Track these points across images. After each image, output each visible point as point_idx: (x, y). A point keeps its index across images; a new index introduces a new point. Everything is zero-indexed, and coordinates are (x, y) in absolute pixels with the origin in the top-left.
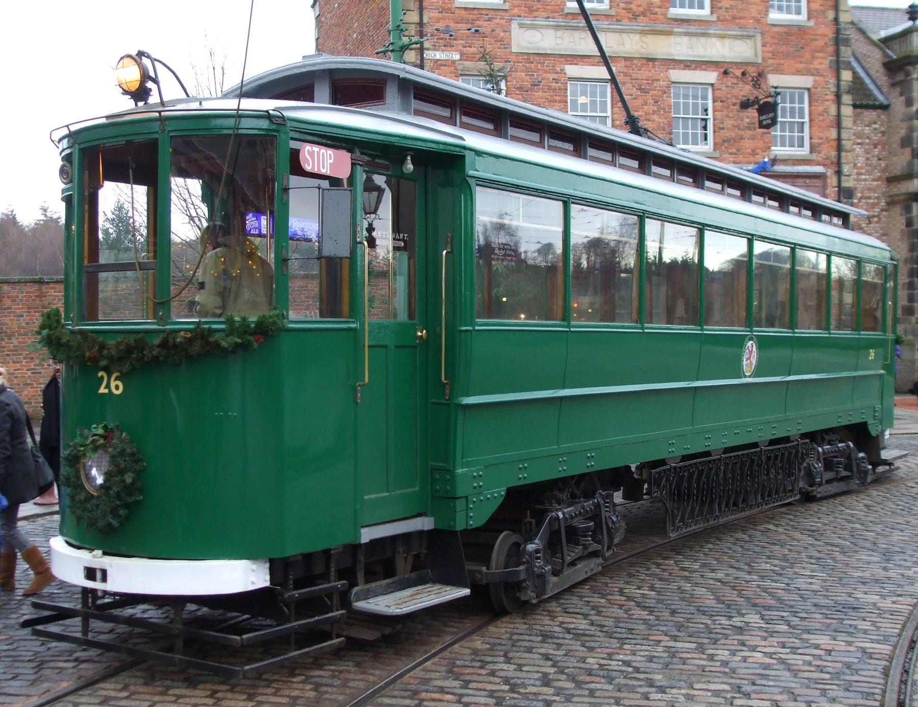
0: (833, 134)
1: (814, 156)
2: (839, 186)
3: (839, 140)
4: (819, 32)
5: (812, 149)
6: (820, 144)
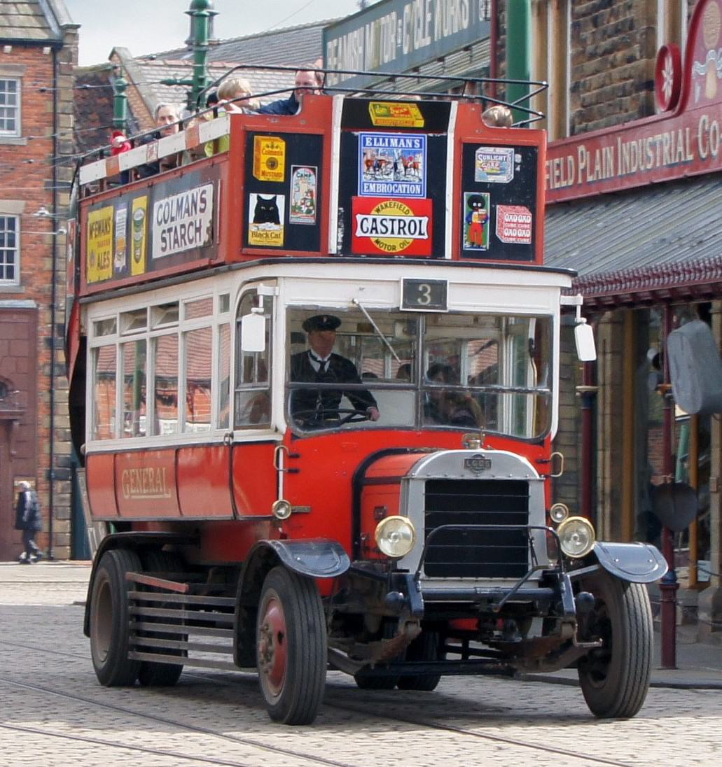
0: (48, 264)
1: (23, 290)
2: (53, 323)
3: (54, 270)
4: (33, 151)
5: (24, 281)
6: (31, 276)
